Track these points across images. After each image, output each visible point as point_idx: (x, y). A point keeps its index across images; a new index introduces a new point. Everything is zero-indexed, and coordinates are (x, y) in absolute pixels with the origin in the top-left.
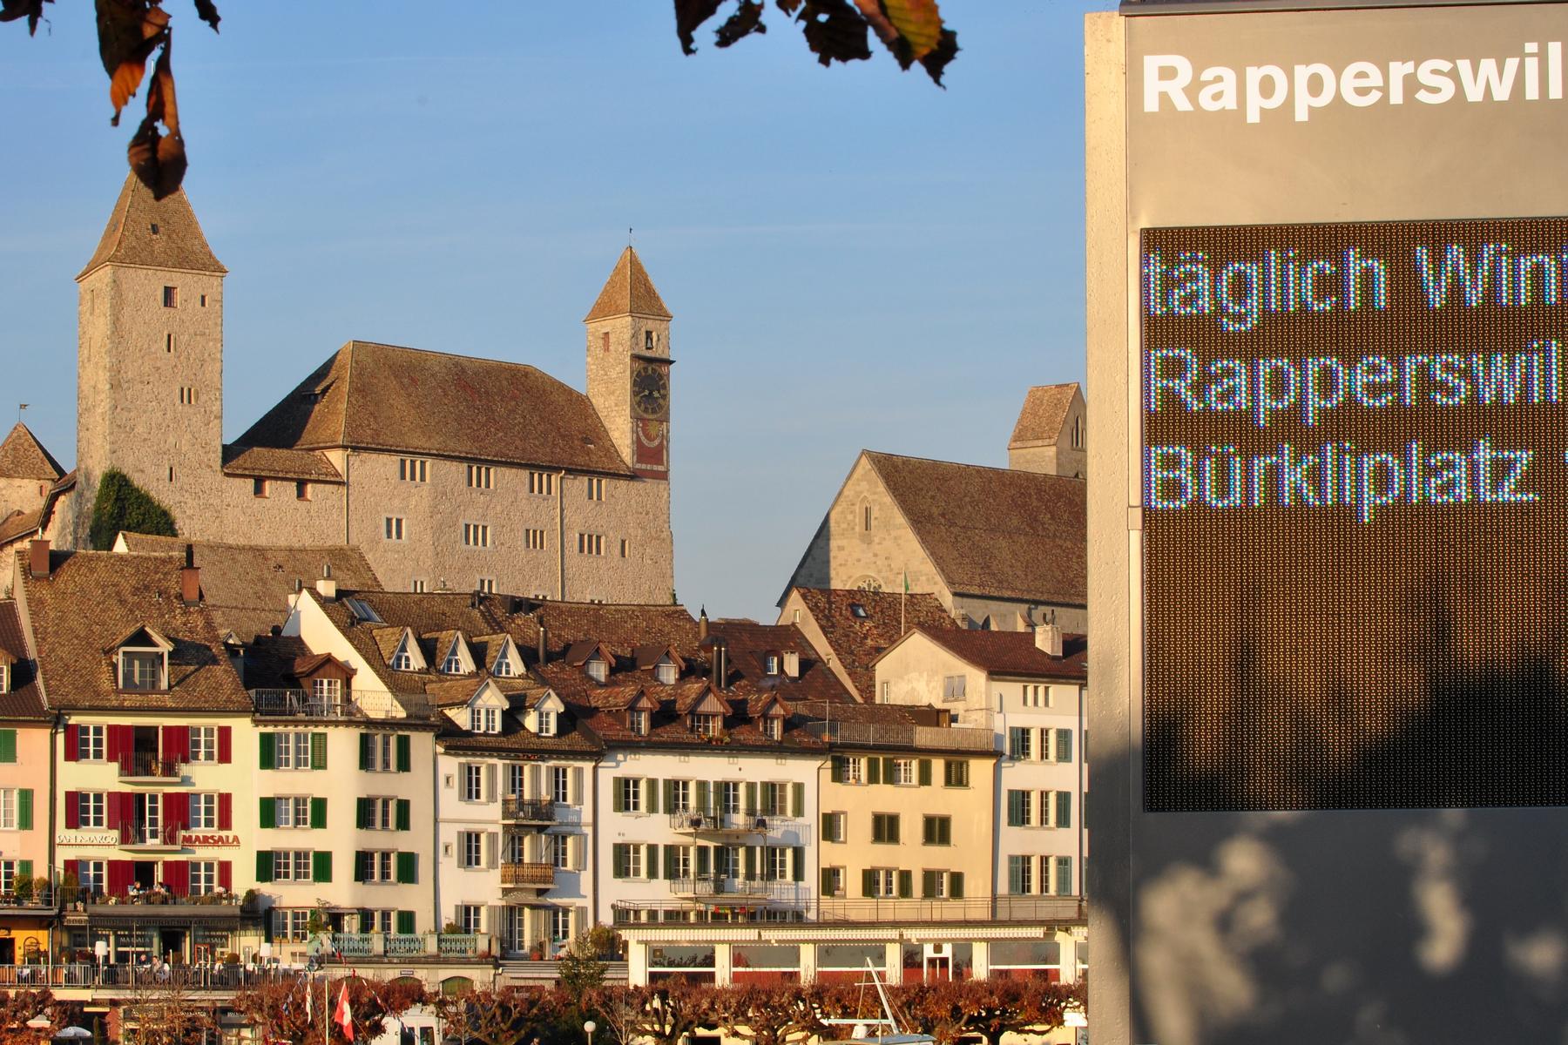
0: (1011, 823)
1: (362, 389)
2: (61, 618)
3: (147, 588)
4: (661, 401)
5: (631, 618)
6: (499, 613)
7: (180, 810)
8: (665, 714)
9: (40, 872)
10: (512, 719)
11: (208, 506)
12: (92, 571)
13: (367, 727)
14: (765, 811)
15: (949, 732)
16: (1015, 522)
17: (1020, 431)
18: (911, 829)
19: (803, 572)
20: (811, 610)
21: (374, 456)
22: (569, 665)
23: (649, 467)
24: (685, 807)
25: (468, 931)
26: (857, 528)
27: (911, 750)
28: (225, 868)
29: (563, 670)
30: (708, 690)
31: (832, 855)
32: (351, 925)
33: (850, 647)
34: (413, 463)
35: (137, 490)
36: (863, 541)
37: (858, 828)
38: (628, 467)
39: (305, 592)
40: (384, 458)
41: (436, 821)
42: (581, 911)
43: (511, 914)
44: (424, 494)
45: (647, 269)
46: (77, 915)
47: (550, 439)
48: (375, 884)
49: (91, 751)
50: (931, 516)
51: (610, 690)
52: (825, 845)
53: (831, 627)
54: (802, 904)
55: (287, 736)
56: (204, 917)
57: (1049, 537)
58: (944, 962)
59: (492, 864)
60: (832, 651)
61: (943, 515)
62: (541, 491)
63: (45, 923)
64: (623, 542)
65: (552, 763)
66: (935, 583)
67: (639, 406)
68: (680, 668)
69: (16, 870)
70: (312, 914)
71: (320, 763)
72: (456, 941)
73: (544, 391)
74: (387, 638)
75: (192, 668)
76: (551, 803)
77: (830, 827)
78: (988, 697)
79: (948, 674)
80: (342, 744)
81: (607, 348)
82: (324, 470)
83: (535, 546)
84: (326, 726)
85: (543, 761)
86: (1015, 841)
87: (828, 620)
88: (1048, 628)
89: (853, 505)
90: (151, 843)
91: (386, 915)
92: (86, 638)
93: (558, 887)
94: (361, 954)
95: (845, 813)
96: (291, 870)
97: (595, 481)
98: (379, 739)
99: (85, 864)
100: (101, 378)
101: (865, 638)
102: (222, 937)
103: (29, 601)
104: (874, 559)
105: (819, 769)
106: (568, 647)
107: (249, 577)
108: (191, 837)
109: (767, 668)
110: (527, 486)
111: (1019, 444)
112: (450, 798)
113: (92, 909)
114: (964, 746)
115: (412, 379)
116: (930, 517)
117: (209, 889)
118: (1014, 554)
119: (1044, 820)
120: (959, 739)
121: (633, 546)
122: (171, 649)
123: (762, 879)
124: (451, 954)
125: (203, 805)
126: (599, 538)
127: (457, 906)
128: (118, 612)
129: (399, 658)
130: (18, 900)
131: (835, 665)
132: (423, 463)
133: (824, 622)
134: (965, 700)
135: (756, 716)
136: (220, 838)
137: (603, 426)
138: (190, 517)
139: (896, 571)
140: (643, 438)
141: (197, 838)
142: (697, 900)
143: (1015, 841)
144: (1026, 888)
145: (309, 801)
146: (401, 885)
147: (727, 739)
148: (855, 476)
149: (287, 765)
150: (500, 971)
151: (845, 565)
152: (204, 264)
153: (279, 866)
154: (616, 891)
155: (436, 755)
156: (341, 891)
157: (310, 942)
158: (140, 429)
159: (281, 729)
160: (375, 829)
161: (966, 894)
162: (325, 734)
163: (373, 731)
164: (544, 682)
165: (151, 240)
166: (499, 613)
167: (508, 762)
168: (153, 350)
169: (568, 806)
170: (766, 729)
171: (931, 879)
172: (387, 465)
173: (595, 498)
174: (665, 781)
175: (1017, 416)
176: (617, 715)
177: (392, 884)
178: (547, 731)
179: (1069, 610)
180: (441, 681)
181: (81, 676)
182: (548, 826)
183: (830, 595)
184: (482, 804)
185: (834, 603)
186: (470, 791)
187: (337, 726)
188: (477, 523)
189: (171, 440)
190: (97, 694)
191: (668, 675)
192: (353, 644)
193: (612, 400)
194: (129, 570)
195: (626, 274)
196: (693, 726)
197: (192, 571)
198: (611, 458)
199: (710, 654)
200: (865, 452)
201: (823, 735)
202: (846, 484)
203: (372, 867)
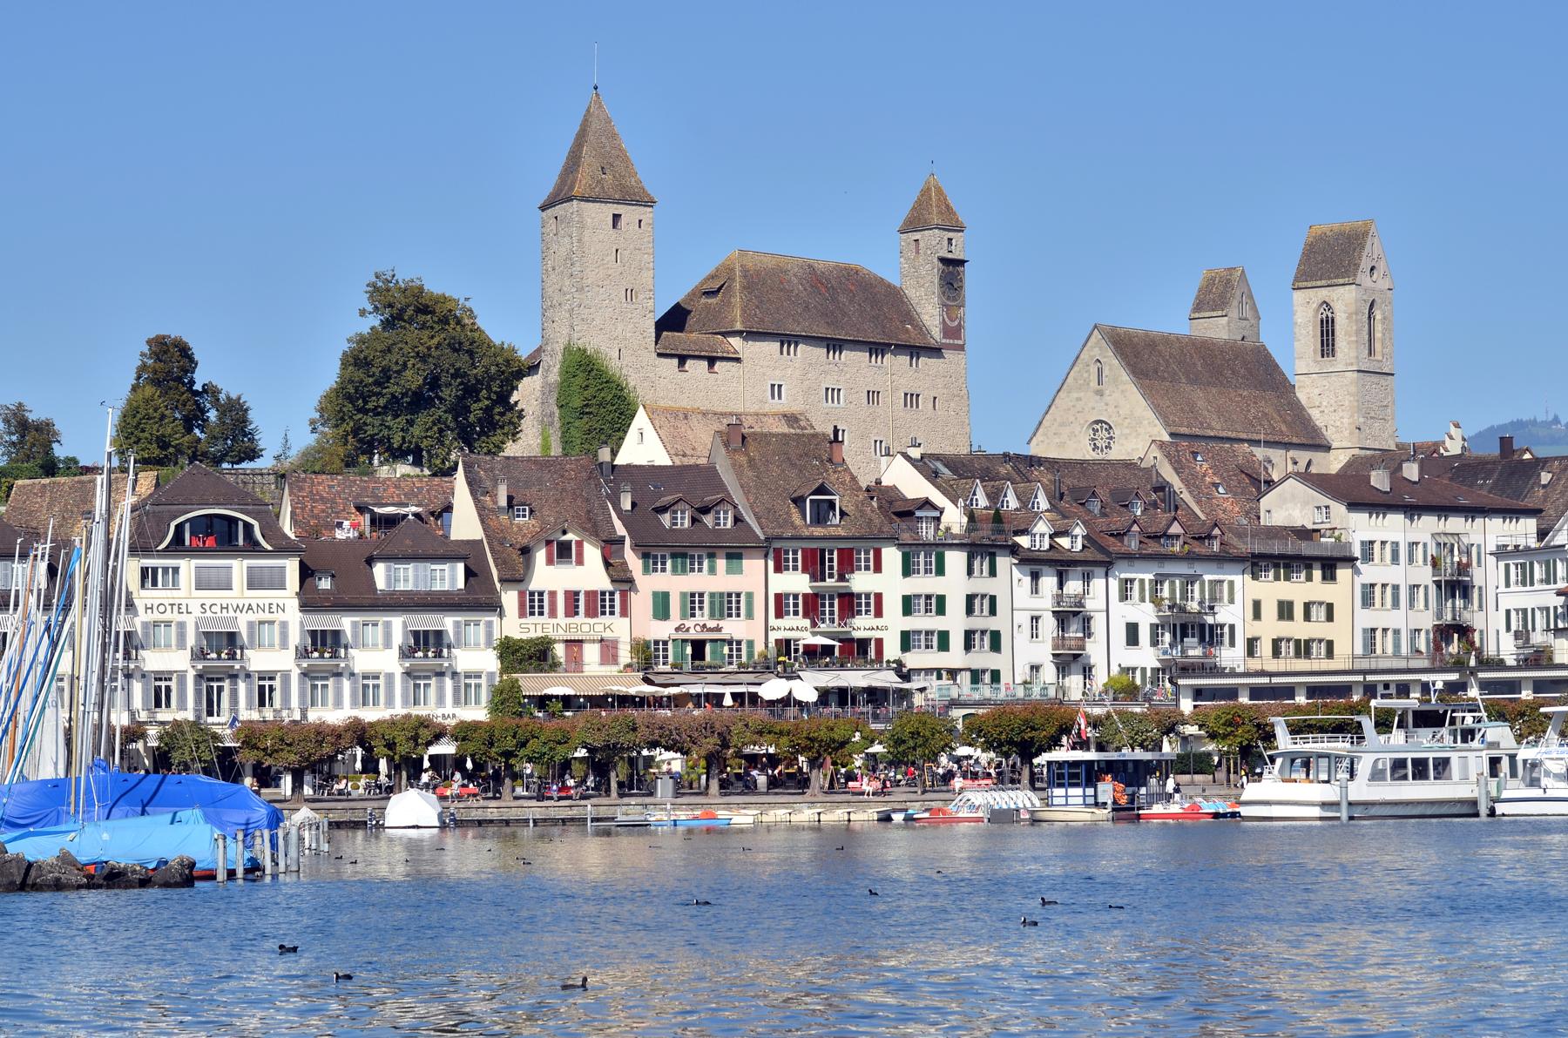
7: (849, 603)
9: (759, 647)
12: (769, 443)
17: (1198, 304)
19: (1048, 417)
22: (1076, 500)
23: (951, 341)
26: (1092, 384)
28: (879, 642)
30: (1175, 519)
32: (964, 678)
37: (1270, 610)
60: (1182, 486)
64: (935, 398)
66: (1155, 426)
80: (955, 560)
81: (918, 252)
86: (1367, 618)
89: (1088, 365)
100: (567, 283)
101: (1205, 476)
103: (734, 465)
104: (1105, 407)
111: (1197, 315)
126: (918, 396)
128: (793, 474)
129: (972, 500)
131: (1186, 496)
140: (947, 319)
143: (1367, 618)
148: (1089, 344)
149: (919, 573)
156: (955, 657)
161: (1335, 652)
164: (1065, 517)
175: (1194, 293)
176: (1119, 536)
177: (986, 652)
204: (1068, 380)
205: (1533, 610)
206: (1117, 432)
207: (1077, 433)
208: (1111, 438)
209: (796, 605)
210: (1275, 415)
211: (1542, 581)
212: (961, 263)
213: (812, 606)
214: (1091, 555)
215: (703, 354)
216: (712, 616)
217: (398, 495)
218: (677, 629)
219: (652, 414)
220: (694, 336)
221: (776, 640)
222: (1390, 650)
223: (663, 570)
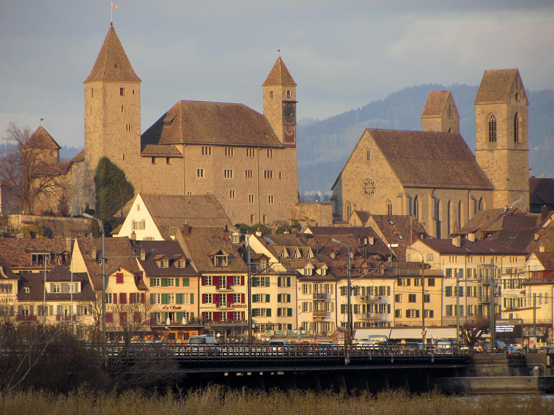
1: (186, 120)
2: (195, 246)
4: (293, 118)
6: (304, 239)
7: (232, 298)
9: (196, 316)
10: (314, 271)
14: (380, 295)
16: (426, 154)
17: (426, 110)
20: (376, 222)
21: (193, 146)
22: (325, 254)
23: (289, 143)
26: (364, 160)
31: (398, 306)
32: (276, 328)
34: (206, 148)
37: (405, 298)
38: (281, 144)
40: (197, 147)
42: (333, 323)
47: (253, 135)
52: (396, 303)
55: (259, 278)
57: (440, 160)
60: (383, 236)
61: (398, 153)
62: (250, 155)
64: (280, 173)
65: (325, 283)
66: (396, 182)
69: (190, 315)
71: (268, 285)
74: (278, 249)
76: (326, 294)
78: (440, 260)
79: (428, 253)
80: (273, 280)
81: (272, 97)
83: (249, 177)
87: (382, 226)
89: (362, 150)
91: (284, 325)
97: (270, 150)
98: (282, 279)
99: (207, 313)
101: (394, 231)
103: (185, 241)
106: (323, 248)
107: (181, 207)
109: (363, 242)
110: (246, 154)
111: (426, 116)
112: (300, 293)
113: (211, 325)
114: (434, 275)
115: (203, 114)
118: (426, 167)
126: (271, 172)
128: (209, 244)
129: (282, 254)
132: (210, 148)
133: (380, 227)
138: (131, 173)
144: (451, 314)
146: (288, 317)
148: (363, 138)
149: (259, 285)
152: (133, 79)
153: (257, 312)
156: (274, 319)
158: (113, 141)
163: (281, 276)
164: (320, 261)
165: (115, 71)
168: (117, 112)
172: (198, 149)
173: (270, 156)
175: (425, 104)
189: (124, 145)
190: (209, 268)
193: (274, 118)
194: (209, 232)
195: (279, 68)
199: (362, 249)
202: (359, 141)
204: (352, 157)
206: (376, 185)
207: (356, 184)
208: (374, 188)
209: (210, 298)
212: (295, 102)
213: (217, 299)
215: (164, 155)
216: (177, 303)
217: (43, 247)
218: (163, 308)
219: (144, 198)
220: (159, 147)
221: (202, 312)
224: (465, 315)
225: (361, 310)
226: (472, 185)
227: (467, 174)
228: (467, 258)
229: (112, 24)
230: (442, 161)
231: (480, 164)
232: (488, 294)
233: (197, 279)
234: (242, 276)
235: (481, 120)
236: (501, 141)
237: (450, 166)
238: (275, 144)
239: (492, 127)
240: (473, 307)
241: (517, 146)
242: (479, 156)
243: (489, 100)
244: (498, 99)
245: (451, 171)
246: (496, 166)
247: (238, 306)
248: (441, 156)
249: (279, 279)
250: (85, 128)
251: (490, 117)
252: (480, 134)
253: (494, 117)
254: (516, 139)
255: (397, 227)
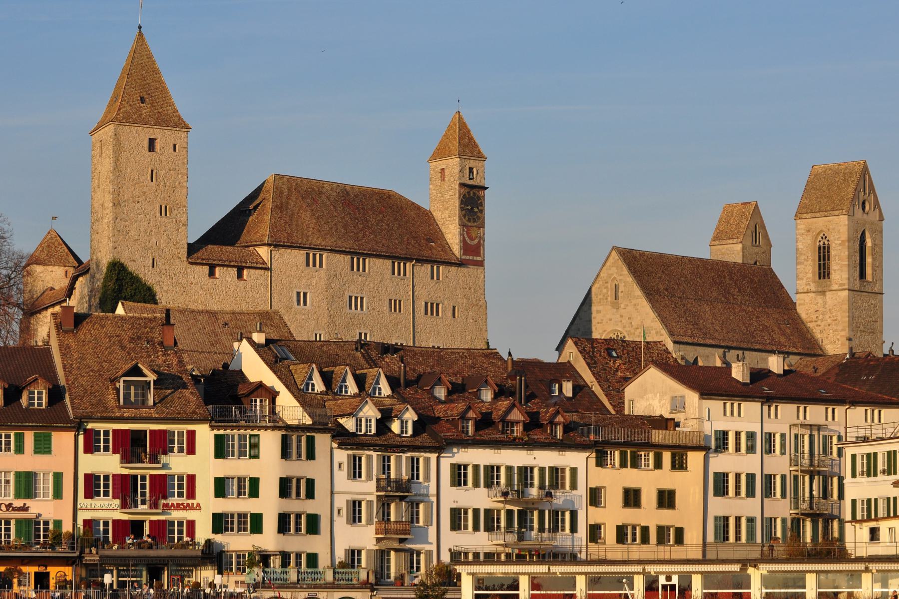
0: (715, 495)
1: (280, 206)
2: (81, 358)
3: (139, 338)
4: (479, 214)
5: (462, 358)
6: (374, 354)
7: (161, 486)
8: (485, 422)
9: (67, 527)
11: (178, 284)
12: (102, 326)
13: (286, 430)
14: (551, 486)
15: (674, 434)
18: (649, 498)
19: (573, 327)
20: (581, 352)
21: (289, 251)
22: (420, 388)
23: (471, 258)
24: (498, 484)
25: (353, 567)
26: (609, 299)
27: (649, 446)
28: (191, 524)
29: (416, 392)
31: (596, 515)
32: (275, 563)
33: (607, 377)
34: (314, 255)
35: (131, 273)
36: (613, 307)
37: (613, 498)
38: (457, 258)
39: (244, 341)
40: (295, 252)
41: (332, 493)
42: (429, 553)
43: (382, 556)
44: (322, 276)
45: (469, 127)
46: (92, 556)
48: (292, 535)
49: (102, 447)
50: (658, 290)
51: (448, 405)
52: (591, 509)
53: (594, 364)
54: (577, 549)
55: (233, 436)
56: (177, 557)
57: (737, 304)
58: (673, 587)
59: (369, 522)
60: (595, 380)
61: (667, 290)
62: (399, 274)
63: (70, 562)
64: (454, 307)
65: (409, 454)
66: (661, 335)
67: (465, 218)
68: (495, 391)
69: (51, 527)
70: (249, 555)
72: (345, 573)
73: (401, 207)
74: (299, 371)
75: (169, 391)
76: (409, 481)
77: (595, 497)
79: (674, 395)
80: (270, 441)
81: (443, 180)
82: (255, 260)
84: (259, 430)
85: (404, 453)
86: (718, 506)
87: (592, 359)
88: (740, 364)
89: (607, 283)
90: (142, 508)
91: (298, 556)
92: (99, 371)
93: (413, 537)
94: (282, 582)
95: (604, 487)
96: (235, 526)
97: (435, 267)
98: (294, 438)
101: (617, 371)
102: (188, 571)
104: (620, 319)
105: (587, 458)
106: (420, 377)
108: (168, 504)
109: (551, 391)
110: (390, 271)
111: (717, 242)
112: (341, 477)
113: (102, 552)
114: (685, 442)
116: (658, 291)
117: (180, 539)
119: (737, 492)
120: (681, 438)
121: (460, 310)
122: (155, 379)
123: (549, 532)
124: (342, 582)
125: (176, 483)
126: (438, 305)
127: (346, 550)
128: (120, 353)
129: (307, 385)
130: (52, 547)
131: (597, 389)
132: (321, 256)
134: (684, 412)
135: (545, 423)
136: (188, 504)
137: (441, 231)
138: (166, 292)
139: (635, 327)
141: (172, 504)
142: (506, 546)
143: (718, 506)
145: (247, 479)
146: (308, 535)
147: (526, 438)
148: (608, 264)
150: (375, 593)
151: (601, 323)
153: (227, 523)
154: (452, 540)
155: (332, 448)
157: (248, 574)
158: (132, 233)
159: (228, 432)
160: (291, 499)
161: (686, 542)
162: (258, 435)
163: (291, 433)
164: (404, 400)
165: (140, 107)
166: (374, 354)
167: (380, 453)
169: (420, 483)
170: (552, 431)
171: (662, 532)
172: (299, 256)
174: (485, 466)
176: (453, 423)
177: (303, 535)
178: (406, 433)
179: (751, 353)
180: (335, 399)
181: (95, 397)
182: (407, 496)
183: (593, 342)
184: (363, 481)
185: (595, 348)
186: (355, 473)
187: (266, 430)
188: (357, 295)
189: (154, 240)
191: (486, 396)
192: (277, 375)
194: (127, 326)
195: (456, 129)
196: (503, 429)
197: (169, 327)
198: (446, 252)
200: (614, 248)
201: (590, 436)
203: (290, 524)
205: (876, 500)
210: (775, 328)
211: (884, 472)
214: (418, 441)
216: (18, 496)
221: (85, 521)
222: (744, 539)
223: (8, 449)
224: (759, 540)
225: (503, 524)
226: (790, 346)
227: (781, 330)
228: (766, 408)
229: (140, 27)
230: (741, 307)
231: (803, 316)
232: (814, 493)
233: (69, 436)
234: (188, 432)
235: (807, 245)
236: (838, 277)
237: (754, 315)
238: (444, 257)
239: (824, 255)
240: (779, 522)
241: (865, 286)
242: (802, 302)
243: (819, 212)
244: (833, 209)
245: (755, 324)
246: (830, 317)
247: (178, 507)
248: (739, 298)
249: (285, 442)
250: (92, 212)
251: (820, 238)
252: (803, 266)
253: (826, 237)
254: (862, 275)
255: (624, 364)
